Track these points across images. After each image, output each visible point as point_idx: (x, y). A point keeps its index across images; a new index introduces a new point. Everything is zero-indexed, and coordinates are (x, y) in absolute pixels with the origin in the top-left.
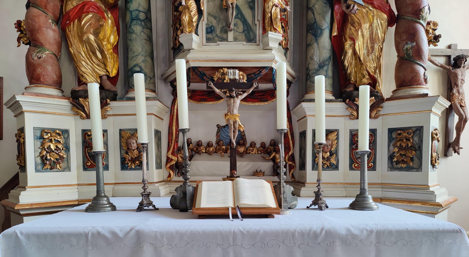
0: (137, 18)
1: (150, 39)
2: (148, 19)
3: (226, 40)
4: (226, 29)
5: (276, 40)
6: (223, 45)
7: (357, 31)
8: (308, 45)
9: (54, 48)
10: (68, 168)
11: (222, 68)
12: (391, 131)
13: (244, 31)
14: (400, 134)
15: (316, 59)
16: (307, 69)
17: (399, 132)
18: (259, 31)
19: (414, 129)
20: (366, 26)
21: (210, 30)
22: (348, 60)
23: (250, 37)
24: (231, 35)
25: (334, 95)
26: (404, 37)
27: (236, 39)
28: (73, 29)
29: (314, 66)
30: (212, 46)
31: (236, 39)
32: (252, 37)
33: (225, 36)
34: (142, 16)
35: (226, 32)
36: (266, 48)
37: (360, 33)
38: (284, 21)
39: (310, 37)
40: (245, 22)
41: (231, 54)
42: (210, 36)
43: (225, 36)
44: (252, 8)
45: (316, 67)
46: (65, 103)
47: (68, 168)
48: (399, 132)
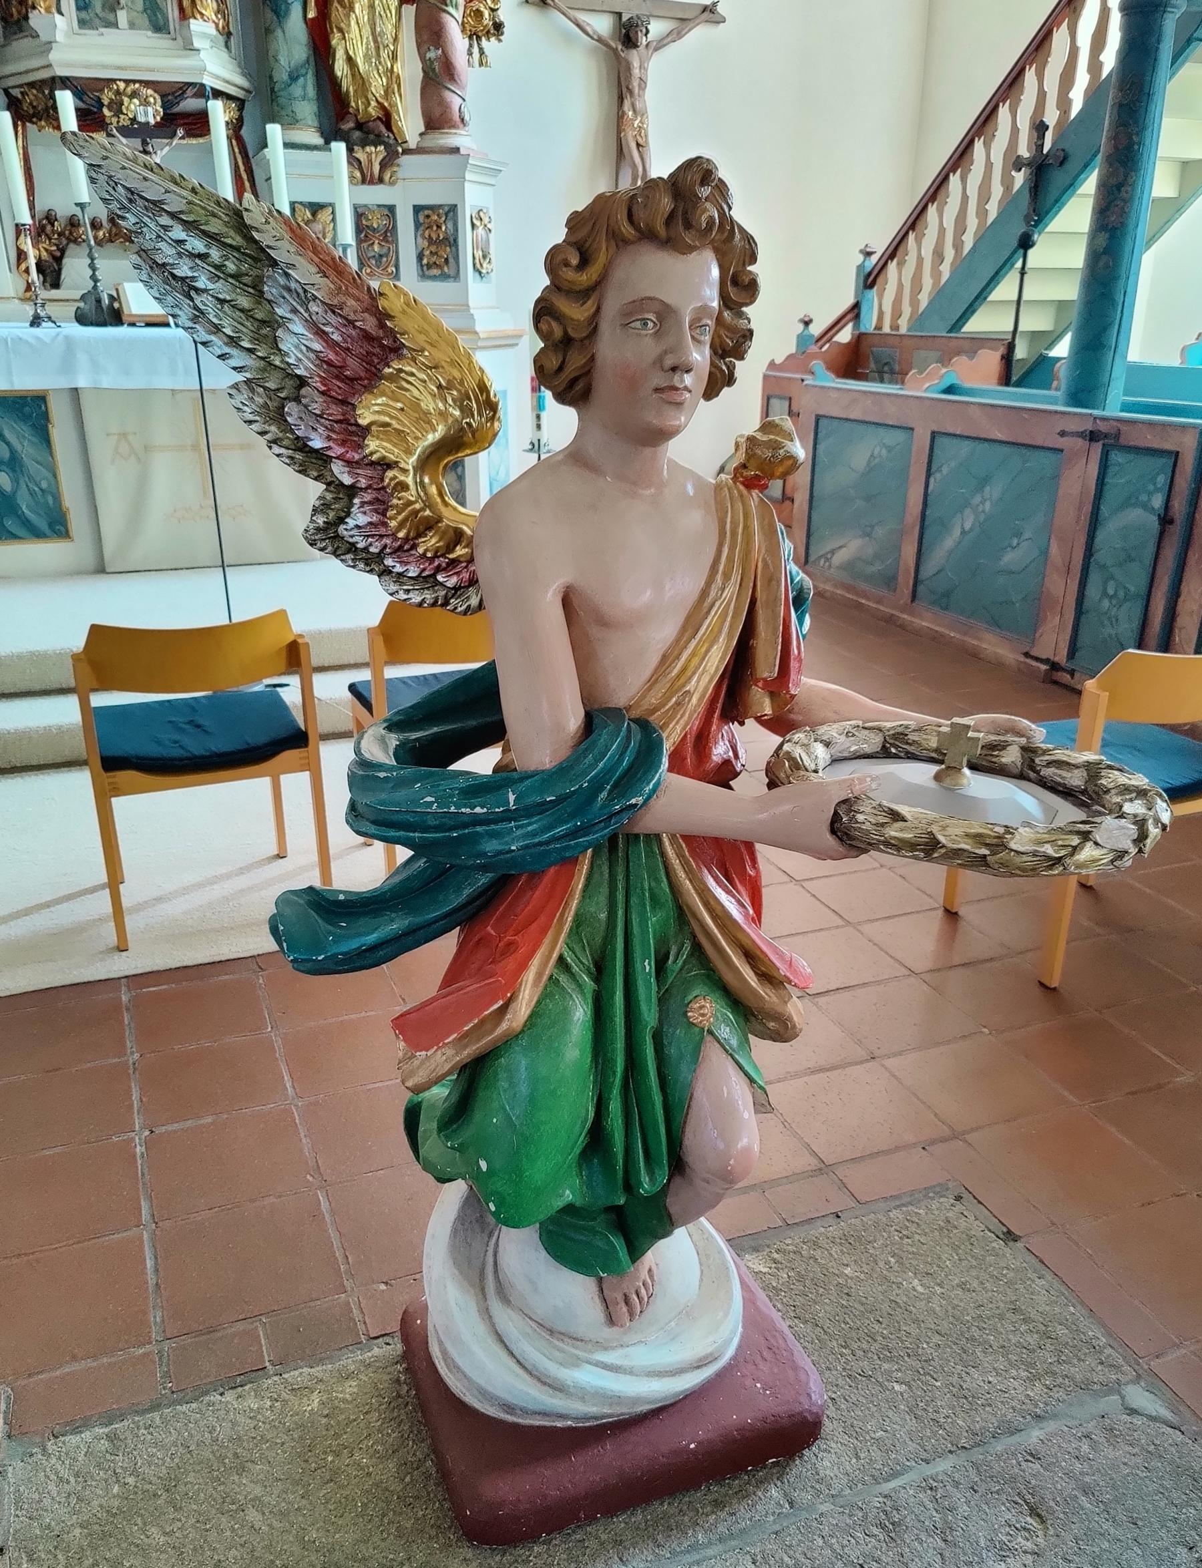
3: (115, 25)
5: (205, 35)
7: (348, 16)
8: (268, 31)
11: (114, 81)
13: (145, 10)
14: (428, 216)
15: (283, 61)
16: (271, 77)
17: (426, 212)
18: (173, 13)
19: (446, 209)
24: (122, 16)
26: (425, 37)
27: (132, 25)
29: (281, 75)
31: (132, 25)
32: (161, 22)
33: (111, 17)
35: (113, 10)
36: (189, 47)
37: (353, 23)
39: (269, 15)
42: (83, 15)
43: (111, 17)
45: (285, 77)
48: (426, 212)
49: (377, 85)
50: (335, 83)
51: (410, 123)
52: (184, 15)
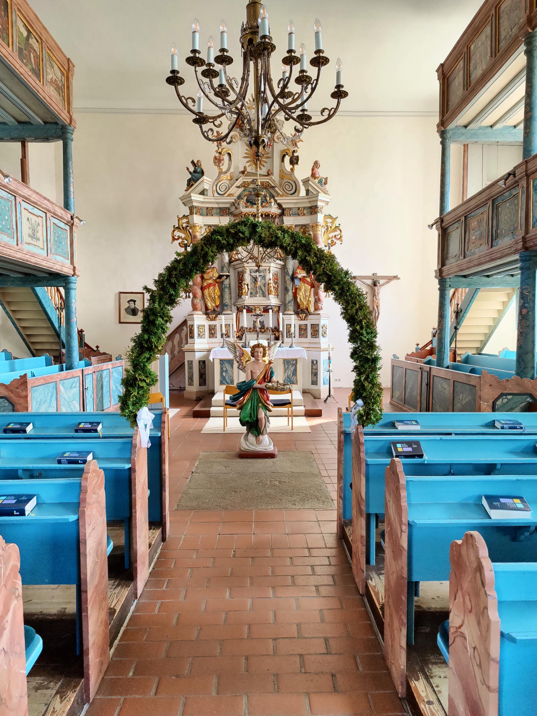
0: (226, 287)
1: (230, 293)
2: (230, 286)
4: (257, 293)
6: (255, 298)
9: (200, 298)
10: (205, 338)
12: (311, 325)
15: (287, 299)
18: (267, 294)
20: (303, 290)
21: (251, 293)
22: (298, 300)
23: (264, 296)
24: (258, 295)
25: (294, 311)
27: (259, 296)
28: (206, 292)
29: (287, 302)
30: (252, 299)
31: (259, 296)
34: (228, 286)
36: (269, 299)
38: (276, 289)
40: (262, 291)
41: (257, 301)
44: (265, 286)
46: (205, 316)
47: (205, 338)
49: (305, 303)
50: (298, 303)
51: (312, 309)
52: (269, 294)
